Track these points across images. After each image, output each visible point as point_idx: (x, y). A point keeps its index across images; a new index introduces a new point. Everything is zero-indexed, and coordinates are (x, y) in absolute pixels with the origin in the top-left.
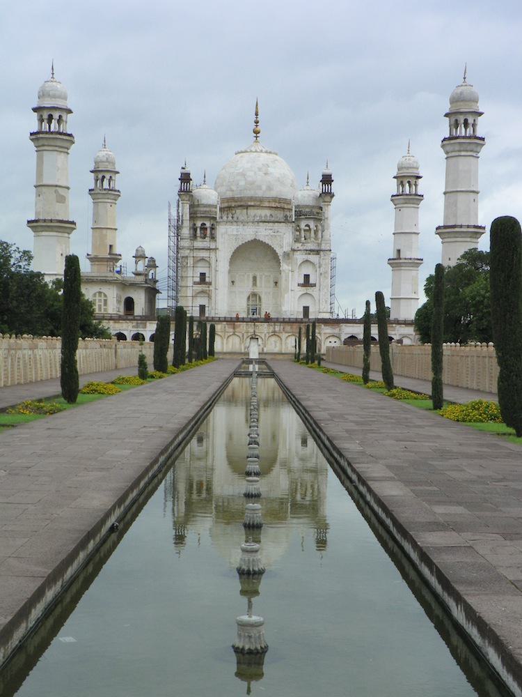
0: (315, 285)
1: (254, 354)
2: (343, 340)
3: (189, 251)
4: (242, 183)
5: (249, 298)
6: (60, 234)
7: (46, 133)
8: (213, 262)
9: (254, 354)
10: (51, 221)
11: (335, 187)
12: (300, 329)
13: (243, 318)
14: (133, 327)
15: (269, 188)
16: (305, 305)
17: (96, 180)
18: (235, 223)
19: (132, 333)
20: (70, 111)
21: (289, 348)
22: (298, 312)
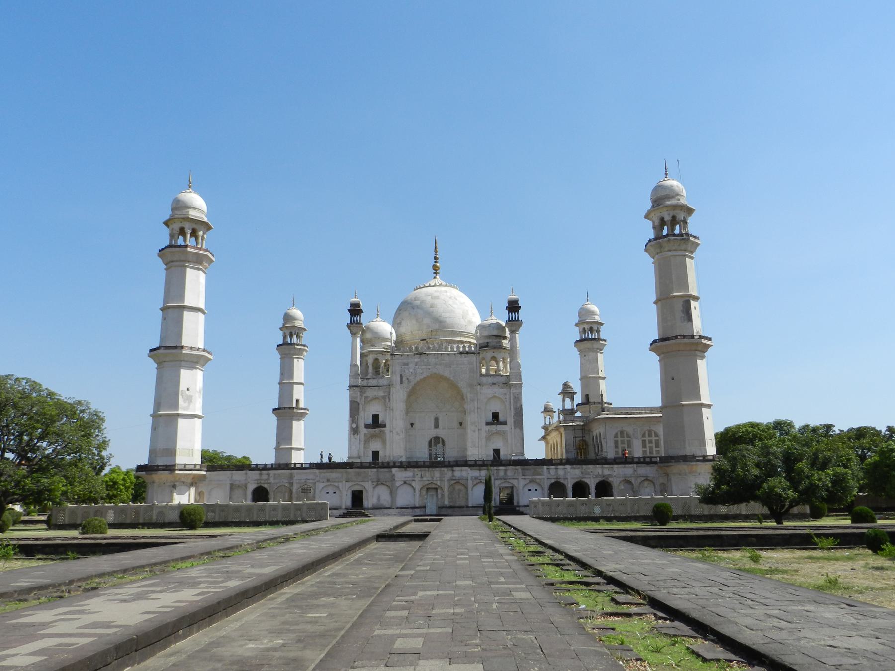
11: (522, 314)
16: (495, 448)
17: (285, 338)
22: (487, 456)
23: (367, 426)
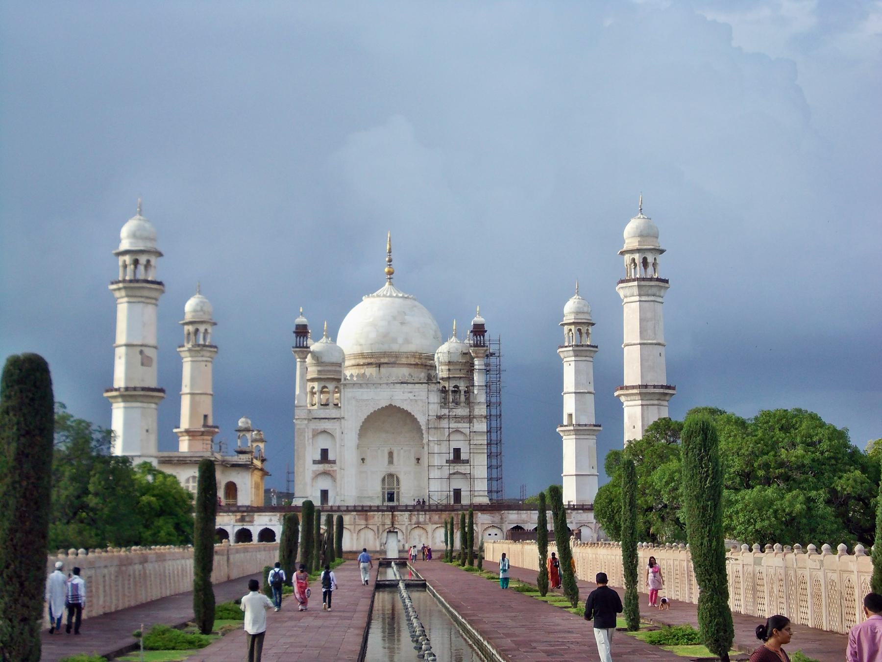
0: (467, 462)
1: (392, 553)
2: (505, 530)
3: (306, 422)
4: (373, 335)
5: (384, 480)
6: (145, 405)
7: (131, 281)
8: (337, 435)
9: (392, 553)
10: (135, 389)
12: (453, 518)
13: (378, 506)
14: (236, 521)
15: (407, 341)
18: (364, 386)
19: (237, 528)
20: (160, 254)
21: (438, 544)
23: (315, 462)
